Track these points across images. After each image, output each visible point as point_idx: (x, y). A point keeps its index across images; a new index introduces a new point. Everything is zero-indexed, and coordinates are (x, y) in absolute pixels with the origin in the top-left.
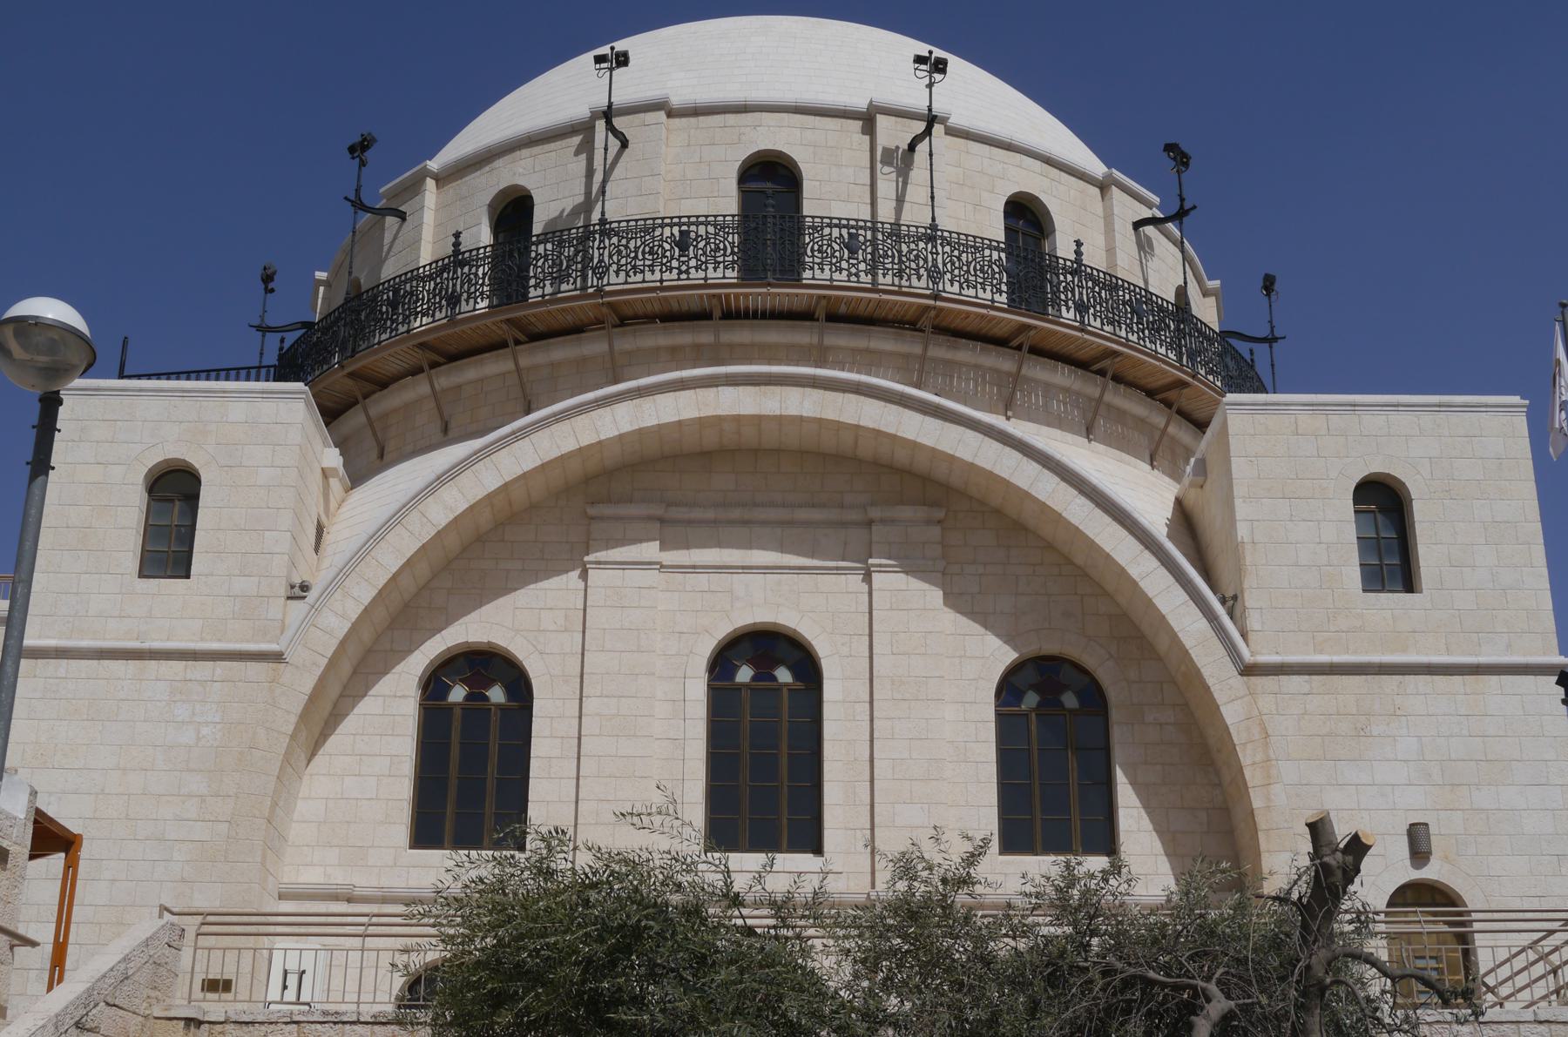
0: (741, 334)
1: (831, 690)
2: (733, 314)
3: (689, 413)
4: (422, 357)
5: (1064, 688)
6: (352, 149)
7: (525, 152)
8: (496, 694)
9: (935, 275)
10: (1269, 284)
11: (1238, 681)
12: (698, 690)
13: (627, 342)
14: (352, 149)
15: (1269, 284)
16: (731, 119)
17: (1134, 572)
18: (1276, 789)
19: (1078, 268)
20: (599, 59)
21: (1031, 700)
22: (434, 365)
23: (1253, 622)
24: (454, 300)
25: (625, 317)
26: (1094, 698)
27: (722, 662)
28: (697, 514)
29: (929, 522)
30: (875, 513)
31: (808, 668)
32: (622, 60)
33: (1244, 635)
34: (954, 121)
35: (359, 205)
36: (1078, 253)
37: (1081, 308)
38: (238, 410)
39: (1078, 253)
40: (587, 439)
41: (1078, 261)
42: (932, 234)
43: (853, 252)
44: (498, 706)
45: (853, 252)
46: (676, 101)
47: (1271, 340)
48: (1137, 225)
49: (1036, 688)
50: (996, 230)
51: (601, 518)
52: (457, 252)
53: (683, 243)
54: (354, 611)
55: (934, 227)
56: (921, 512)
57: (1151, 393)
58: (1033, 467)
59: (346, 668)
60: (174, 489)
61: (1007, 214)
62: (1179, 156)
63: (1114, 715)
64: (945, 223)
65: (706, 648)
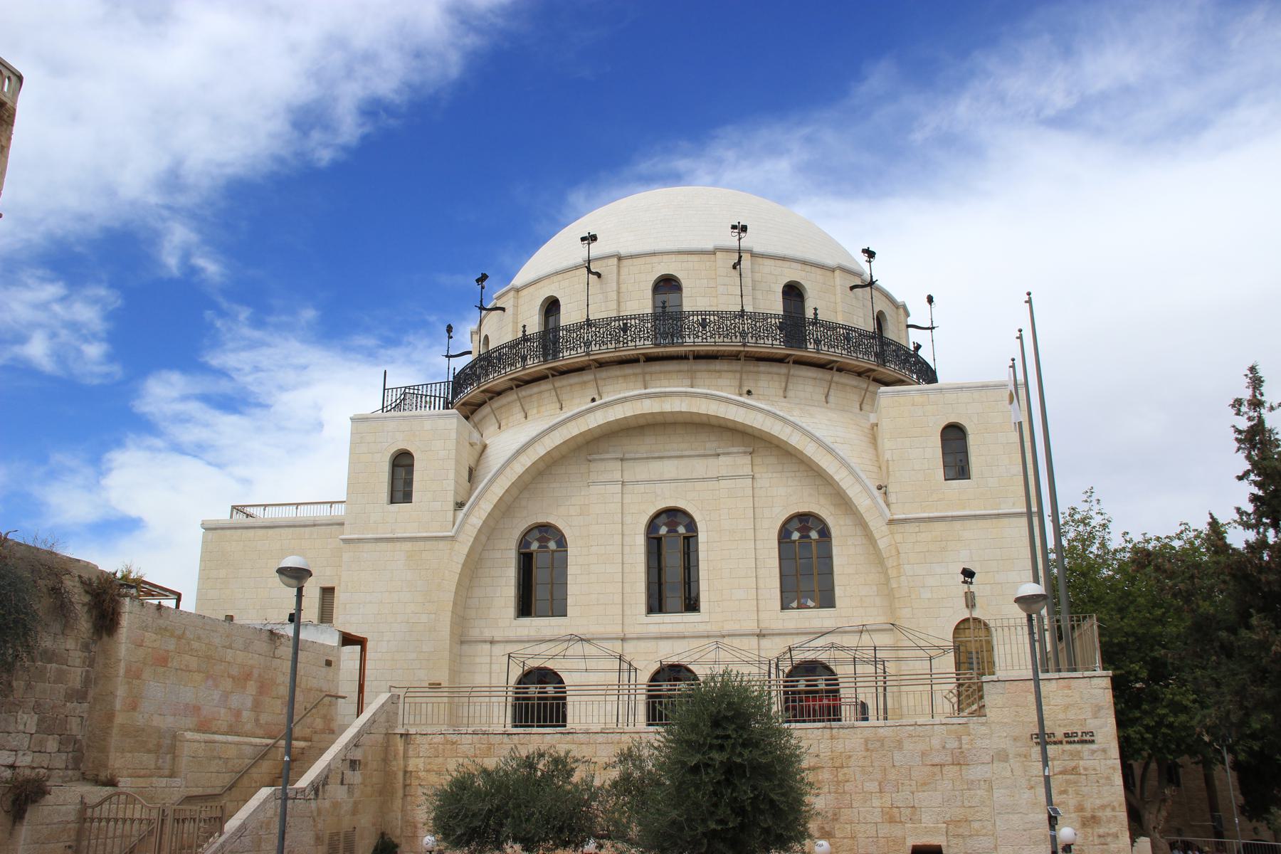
0: (656, 367)
1: (702, 537)
2: (650, 359)
3: (629, 414)
4: (513, 384)
5: (810, 529)
6: (478, 281)
7: (555, 278)
8: (552, 545)
9: (743, 334)
10: (930, 300)
11: (885, 528)
12: (640, 540)
13: (603, 373)
14: (478, 281)
15: (930, 300)
16: (648, 259)
17: (837, 478)
18: (903, 578)
19: (815, 322)
20: (583, 239)
21: (796, 536)
22: (518, 386)
23: (892, 498)
24: (524, 359)
25: (601, 364)
26: (825, 533)
27: (652, 525)
28: (638, 456)
29: (745, 453)
30: (719, 451)
31: (692, 525)
32: (593, 238)
33: (888, 505)
34: (757, 249)
35: (482, 308)
36: (816, 314)
37: (817, 342)
38: (428, 425)
39: (816, 314)
40: (584, 429)
41: (816, 318)
42: (742, 313)
43: (704, 327)
44: (553, 551)
45: (704, 327)
46: (623, 252)
47: (932, 328)
48: (852, 288)
49: (798, 530)
50: (775, 305)
51: (595, 460)
52: (524, 335)
53: (625, 329)
54: (484, 516)
55: (743, 311)
56: (742, 449)
57: (859, 374)
58: (788, 429)
59: (483, 539)
60: (402, 463)
61: (784, 293)
62: (870, 254)
63: (834, 542)
64: (748, 309)
65: (644, 520)
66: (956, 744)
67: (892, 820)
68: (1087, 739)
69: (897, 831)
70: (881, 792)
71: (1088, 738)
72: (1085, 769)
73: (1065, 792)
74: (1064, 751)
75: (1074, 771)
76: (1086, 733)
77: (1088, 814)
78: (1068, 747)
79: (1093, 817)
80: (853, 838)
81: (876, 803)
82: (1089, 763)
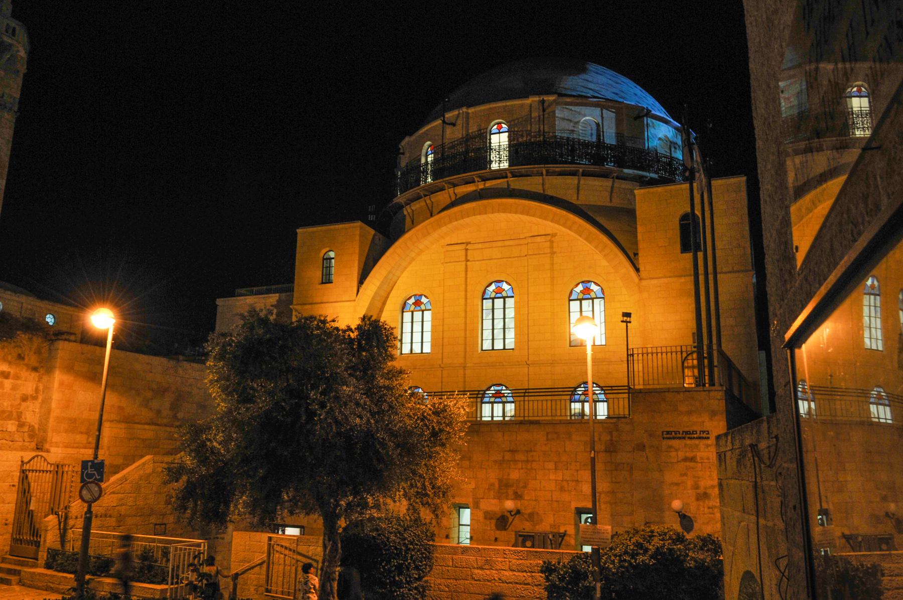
66: (609, 438)
67: (562, 489)
68: (703, 436)
69: (566, 497)
70: (556, 469)
71: (705, 435)
72: (702, 458)
73: (685, 475)
74: (686, 445)
75: (692, 459)
76: (704, 432)
77: (701, 491)
78: (689, 442)
79: (705, 493)
80: (536, 500)
81: (552, 477)
82: (704, 455)
